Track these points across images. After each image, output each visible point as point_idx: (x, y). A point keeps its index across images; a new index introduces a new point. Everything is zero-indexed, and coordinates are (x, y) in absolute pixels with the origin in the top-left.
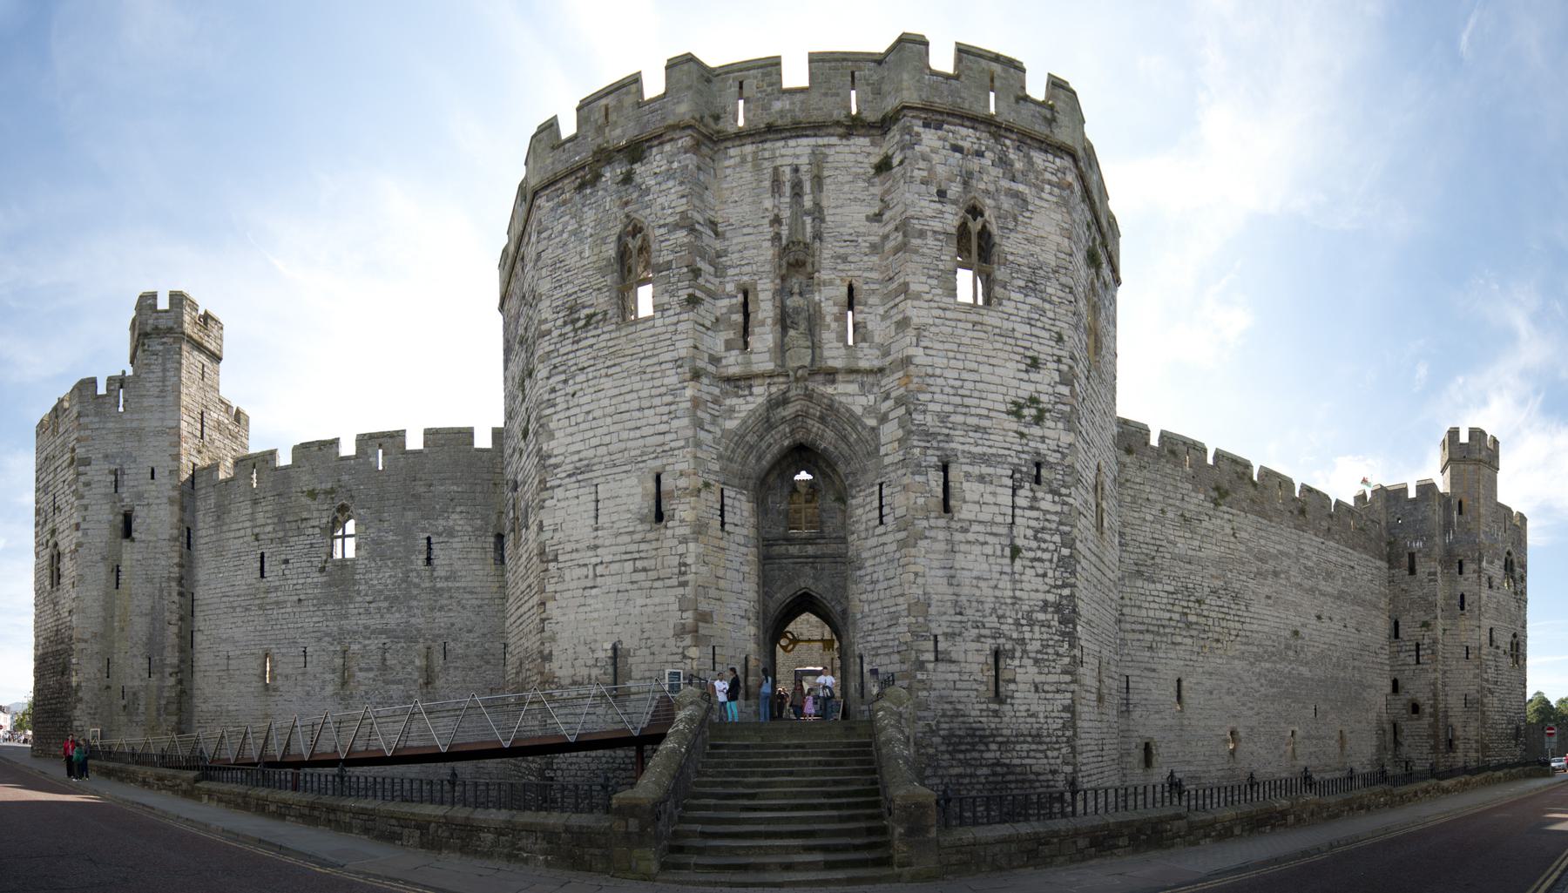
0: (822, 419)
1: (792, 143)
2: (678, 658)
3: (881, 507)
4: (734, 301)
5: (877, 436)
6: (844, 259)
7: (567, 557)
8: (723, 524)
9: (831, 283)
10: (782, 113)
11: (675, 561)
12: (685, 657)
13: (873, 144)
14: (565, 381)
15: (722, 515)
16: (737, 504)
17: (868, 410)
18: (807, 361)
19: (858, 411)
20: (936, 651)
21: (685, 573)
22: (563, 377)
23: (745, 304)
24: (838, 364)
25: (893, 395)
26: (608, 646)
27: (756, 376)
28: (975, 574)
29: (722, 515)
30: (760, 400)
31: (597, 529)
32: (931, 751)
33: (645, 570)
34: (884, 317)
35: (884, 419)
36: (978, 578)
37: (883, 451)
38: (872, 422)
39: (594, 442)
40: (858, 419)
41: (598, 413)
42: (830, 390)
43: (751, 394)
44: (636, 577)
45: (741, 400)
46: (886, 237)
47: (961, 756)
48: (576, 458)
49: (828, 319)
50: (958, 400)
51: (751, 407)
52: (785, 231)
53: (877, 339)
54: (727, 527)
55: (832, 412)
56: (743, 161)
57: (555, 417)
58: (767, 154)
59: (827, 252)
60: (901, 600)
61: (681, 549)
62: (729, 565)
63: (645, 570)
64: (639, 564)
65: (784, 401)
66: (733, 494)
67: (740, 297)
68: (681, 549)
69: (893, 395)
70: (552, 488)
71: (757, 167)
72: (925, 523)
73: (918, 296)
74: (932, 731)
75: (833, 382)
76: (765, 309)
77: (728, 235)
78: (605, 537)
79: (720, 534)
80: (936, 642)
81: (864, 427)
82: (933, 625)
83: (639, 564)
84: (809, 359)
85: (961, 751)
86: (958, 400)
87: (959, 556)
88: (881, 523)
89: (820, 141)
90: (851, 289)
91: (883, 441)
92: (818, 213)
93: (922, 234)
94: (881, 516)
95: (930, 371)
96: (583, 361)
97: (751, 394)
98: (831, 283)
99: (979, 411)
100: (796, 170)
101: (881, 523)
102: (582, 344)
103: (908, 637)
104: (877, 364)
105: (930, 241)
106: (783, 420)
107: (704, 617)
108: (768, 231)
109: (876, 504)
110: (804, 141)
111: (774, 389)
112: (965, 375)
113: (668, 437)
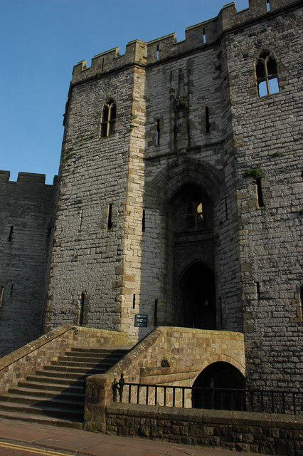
0: (196, 170)
1: (179, 61)
2: (113, 301)
4: (153, 125)
5: (223, 173)
6: (203, 98)
7: (66, 245)
9: (197, 109)
10: (174, 52)
13: (214, 50)
14: (75, 162)
15: (143, 224)
17: (218, 162)
18: (186, 146)
19: (213, 163)
20: (259, 293)
21: (120, 255)
22: (74, 160)
23: (158, 126)
24: (201, 143)
25: (229, 152)
26: (80, 293)
27: (162, 156)
28: (282, 240)
30: (164, 166)
31: (80, 232)
32: (257, 361)
33: (101, 253)
34: (223, 117)
35: (225, 164)
36: (284, 242)
37: (226, 180)
38: (220, 167)
39: (83, 189)
40: (213, 167)
41: (87, 177)
42: (198, 156)
43: (160, 164)
44: (96, 256)
45: (155, 168)
46: (222, 83)
47: (279, 365)
48: (75, 196)
49: (196, 124)
50: (263, 144)
51: (159, 170)
52: (175, 94)
53: (221, 128)
54: (146, 230)
55: (200, 166)
56: (159, 71)
57: (69, 177)
58: (169, 67)
59: (194, 99)
63: (101, 253)
64: (98, 250)
65: (176, 165)
67: (156, 123)
69: (229, 152)
70: (63, 210)
71: (164, 73)
73: (238, 103)
74: (257, 347)
75: (200, 152)
76: (166, 127)
77: (152, 99)
78: (84, 235)
80: (258, 286)
81: (216, 170)
82: (255, 276)
83: (98, 250)
84: (186, 144)
85: (278, 362)
86: (263, 144)
87: (271, 231)
89: (191, 57)
90: (207, 109)
91: (226, 175)
92: (190, 84)
93: (236, 77)
95: (245, 135)
96: (84, 153)
97: (160, 164)
98: (197, 109)
99: (276, 146)
100: (180, 70)
102: (83, 146)
104: (221, 139)
105: (242, 78)
106: (177, 174)
108: (168, 95)
110: (184, 59)
111: (170, 161)
112: (266, 130)
113: (117, 187)
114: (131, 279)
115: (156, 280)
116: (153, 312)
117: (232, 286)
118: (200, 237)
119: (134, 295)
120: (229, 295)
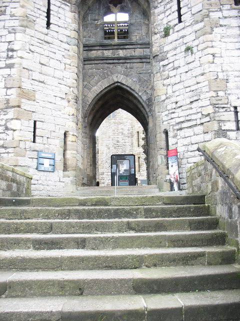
3: (179, 9)
8: (48, 24)
11: (5, 46)
12: (7, 129)
15: (48, 17)
16: (60, 10)
21: (12, 57)
29: (48, 17)
60: (200, 79)
61: (10, 37)
62: (52, 55)
66: (59, 4)
68: (10, 37)
72: (219, 14)
79: (45, 30)
88: (180, 21)
94: (180, 16)
101: (180, 21)
103: (210, 110)
107: (25, 94)
109: (175, 7)
114: (103, 54)
115: (65, 103)
116: (62, 150)
117: (194, 111)
118: (121, 53)
119: (35, 122)
120: (184, 125)
